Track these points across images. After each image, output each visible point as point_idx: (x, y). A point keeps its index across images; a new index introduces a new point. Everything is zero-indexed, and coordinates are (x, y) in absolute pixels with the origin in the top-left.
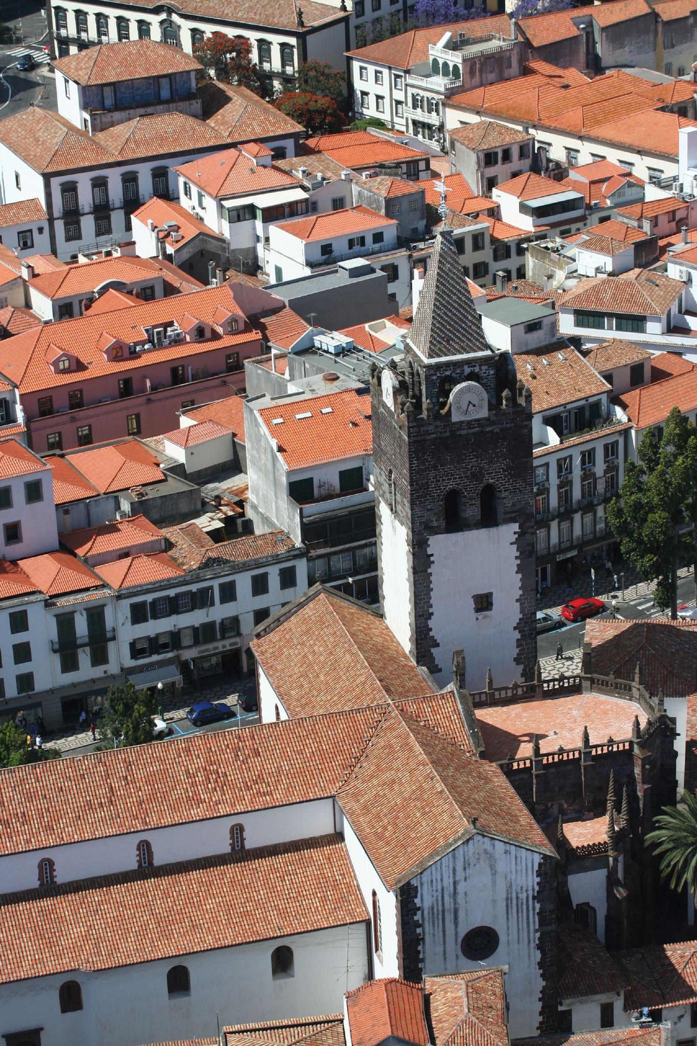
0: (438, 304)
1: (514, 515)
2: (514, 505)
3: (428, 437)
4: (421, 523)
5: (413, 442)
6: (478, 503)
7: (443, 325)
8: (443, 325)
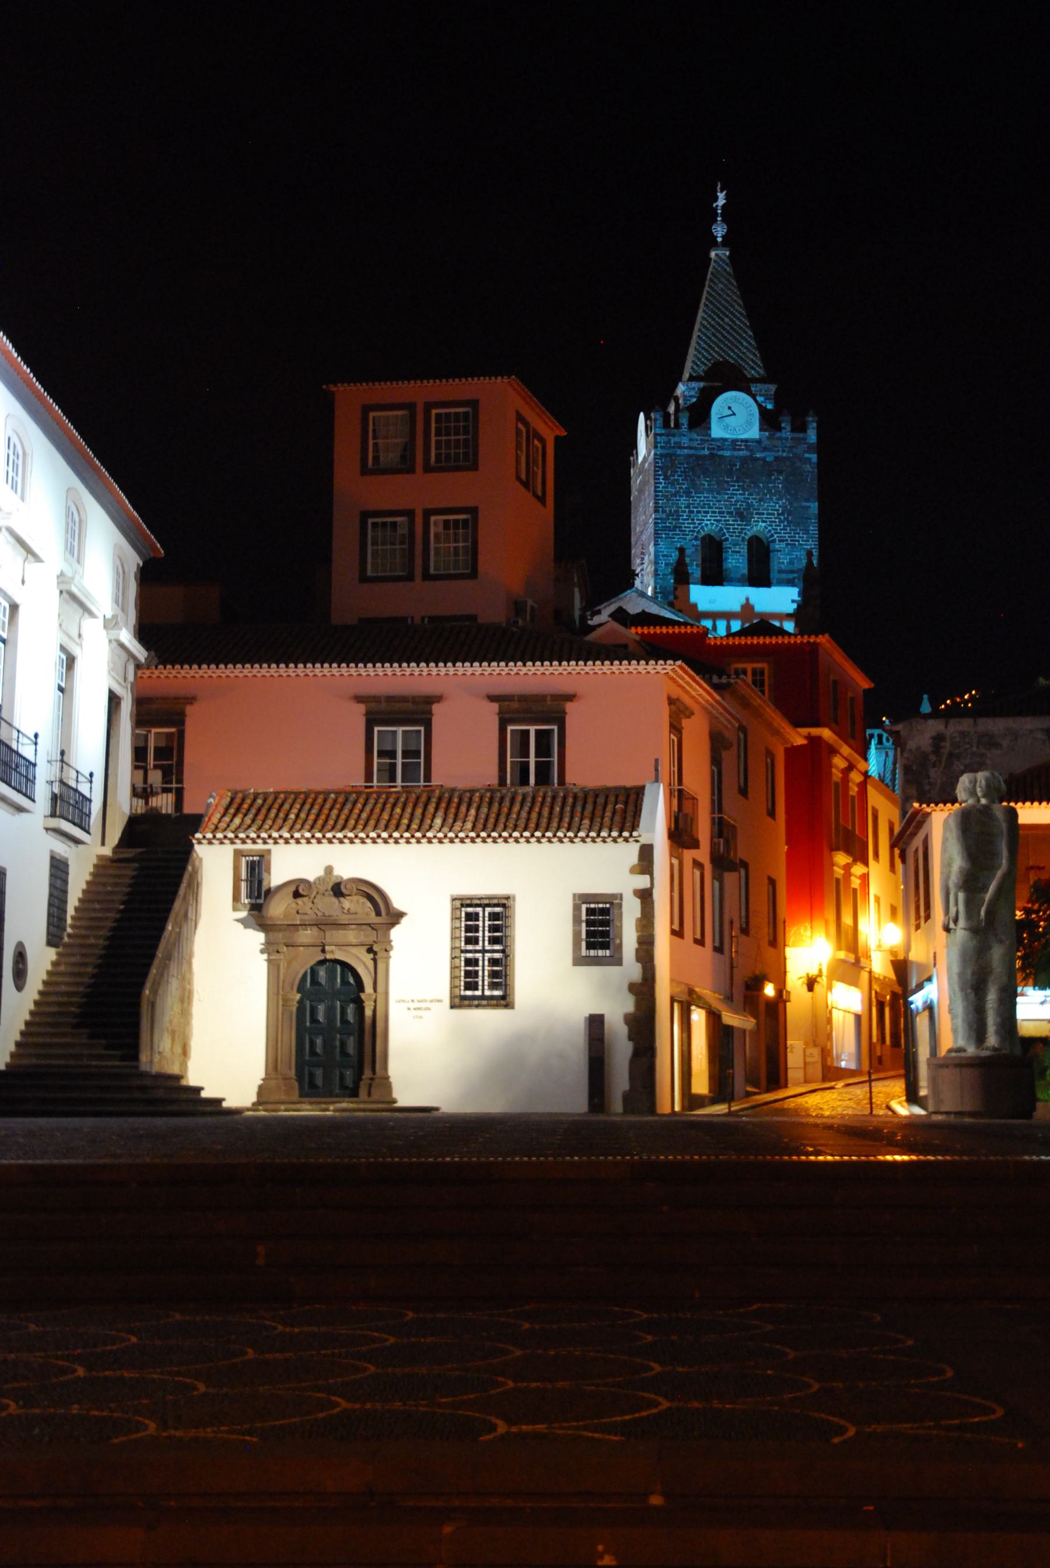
0: (705, 323)
4: (666, 564)
6: (745, 551)
7: (710, 346)
8: (710, 346)
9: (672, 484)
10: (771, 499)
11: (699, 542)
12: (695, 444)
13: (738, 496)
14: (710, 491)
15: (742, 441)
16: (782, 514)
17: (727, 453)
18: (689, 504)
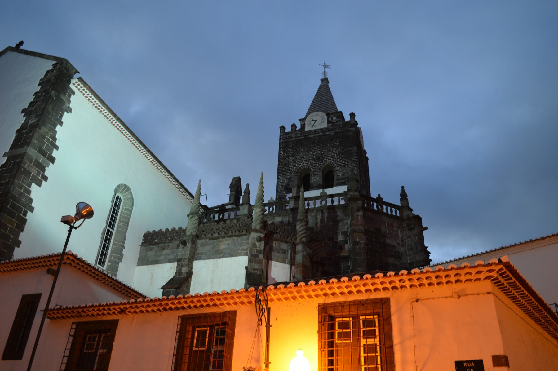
1: (343, 181)
2: (343, 175)
3: (290, 140)
4: (282, 186)
10: (333, 150)
12: (298, 135)
13: (317, 151)
15: (319, 129)
17: (312, 136)
18: (294, 160)
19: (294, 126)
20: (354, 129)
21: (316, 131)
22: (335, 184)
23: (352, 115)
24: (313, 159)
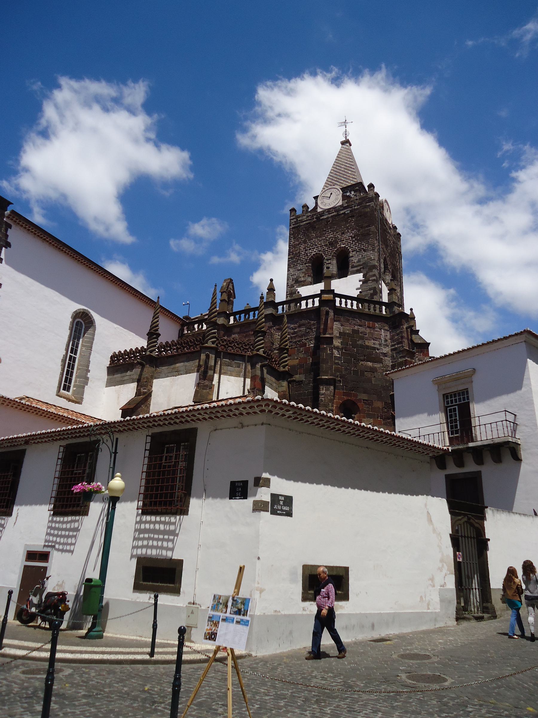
1: (359, 268)
2: (359, 261)
3: (301, 224)
5: (293, 228)
6: (334, 262)
9: (298, 240)
11: (310, 265)
13: (330, 236)
14: (317, 237)
16: (354, 237)
17: (325, 217)
18: (305, 248)
19: (305, 207)
20: (372, 204)
21: (329, 211)
22: (349, 273)
23: (371, 186)
24: (326, 245)
